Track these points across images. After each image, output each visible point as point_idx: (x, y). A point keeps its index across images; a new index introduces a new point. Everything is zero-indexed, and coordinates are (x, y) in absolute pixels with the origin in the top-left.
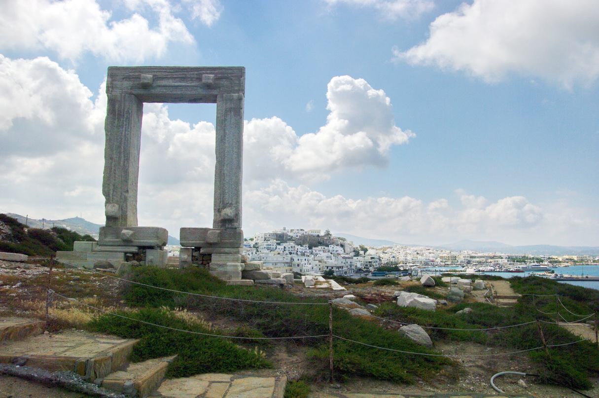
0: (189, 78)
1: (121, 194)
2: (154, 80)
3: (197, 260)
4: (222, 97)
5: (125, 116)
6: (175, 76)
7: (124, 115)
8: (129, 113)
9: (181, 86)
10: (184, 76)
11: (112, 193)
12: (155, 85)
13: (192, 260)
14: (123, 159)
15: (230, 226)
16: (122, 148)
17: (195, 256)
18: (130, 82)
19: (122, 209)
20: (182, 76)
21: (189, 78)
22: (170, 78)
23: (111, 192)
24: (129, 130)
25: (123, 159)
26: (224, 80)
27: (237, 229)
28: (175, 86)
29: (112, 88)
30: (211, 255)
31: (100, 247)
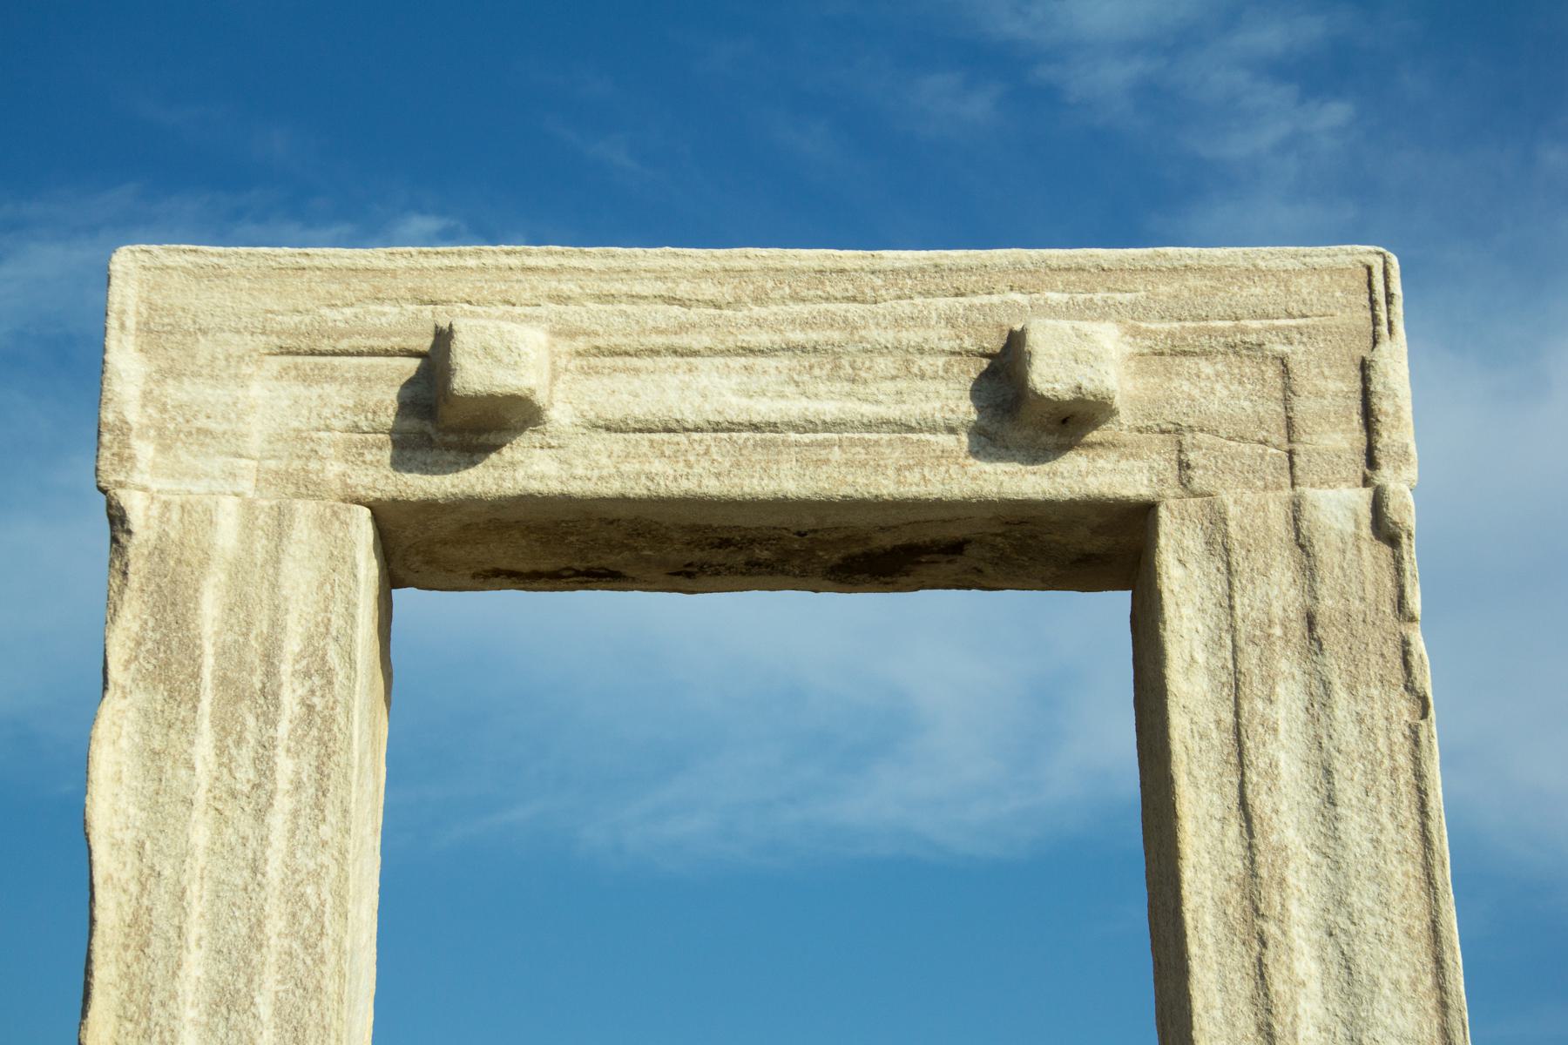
0: (884, 350)
2: (555, 377)
4: (1217, 520)
6: (763, 339)
7: (270, 695)
8: (327, 675)
9: (809, 426)
10: (836, 336)
12: (559, 414)
16: (265, 1010)
18: (330, 389)
20: (814, 336)
21: (884, 350)
22: (713, 352)
24: (325, 830)
26: (1206, 368)
28: (755, 427)
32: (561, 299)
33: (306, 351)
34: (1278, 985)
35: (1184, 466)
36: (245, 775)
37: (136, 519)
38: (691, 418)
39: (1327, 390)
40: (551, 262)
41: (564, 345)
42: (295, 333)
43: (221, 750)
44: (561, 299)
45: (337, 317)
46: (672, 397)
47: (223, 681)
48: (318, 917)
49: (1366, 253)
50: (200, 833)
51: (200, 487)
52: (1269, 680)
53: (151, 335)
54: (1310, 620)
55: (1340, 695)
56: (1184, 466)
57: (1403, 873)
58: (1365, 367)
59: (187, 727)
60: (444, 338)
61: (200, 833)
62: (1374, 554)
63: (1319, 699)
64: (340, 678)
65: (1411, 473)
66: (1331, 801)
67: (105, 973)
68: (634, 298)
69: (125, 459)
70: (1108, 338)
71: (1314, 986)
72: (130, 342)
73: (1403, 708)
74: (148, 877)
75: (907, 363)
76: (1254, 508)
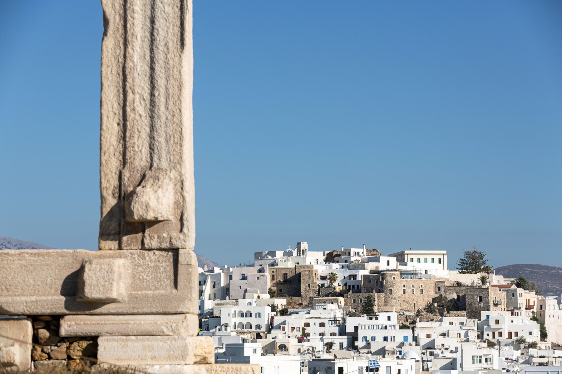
3: (50, 358)
13: (33, 359)
15: (155, 244)
27: (181, 251)
30: (93, 340)
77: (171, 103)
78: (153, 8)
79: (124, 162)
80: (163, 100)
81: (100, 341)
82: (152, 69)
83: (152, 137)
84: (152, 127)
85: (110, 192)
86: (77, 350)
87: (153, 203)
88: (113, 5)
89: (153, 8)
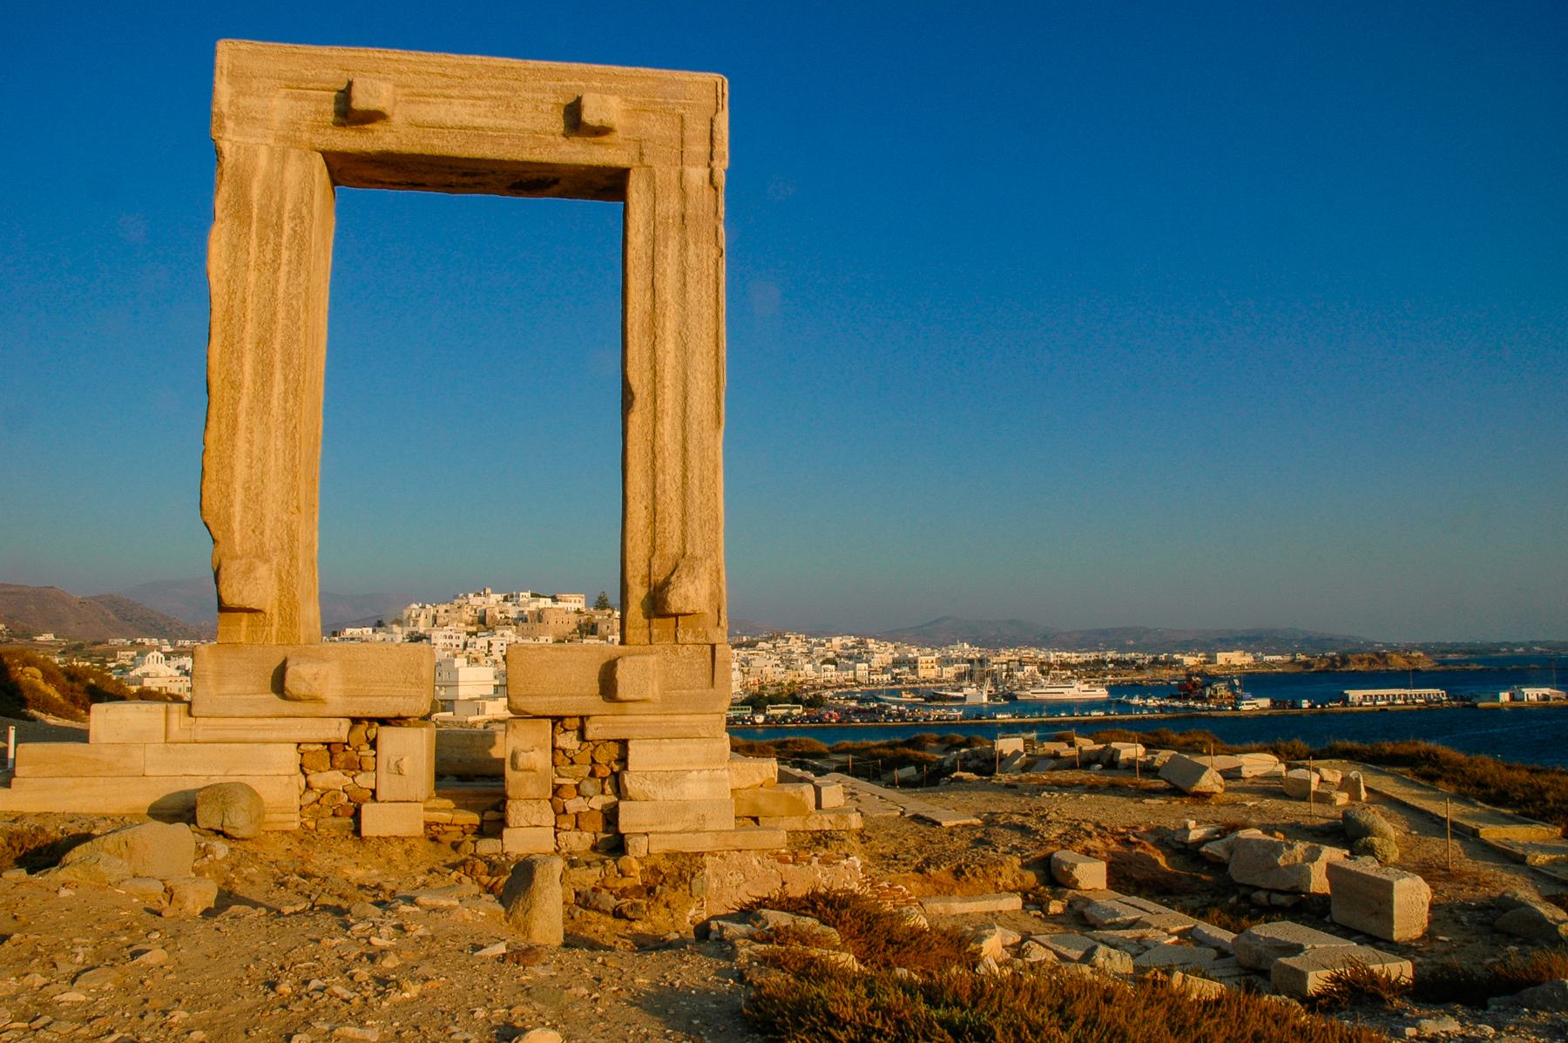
1: (277, 519)
2: (396, 102)
3: (573, 763)
4: (652, 176)
5: (287, 228)
6: (480, 93)
8: (302, 219)
11: (238, 518)
12: (397, 119)
13: (554, 764)
14: (278, 387)
16: (277, 347)
17: (564, 751)
18: (305, 104)
19: (281, 579)
22: (459, 97)
23: (237, 509)
24: (301, 279)
25: (278, 387)
29: (238, 121)
30: (623, 744)
31: (201, 721)
32: (401, 73)
33: (296, 86)
34: (659, 352)
35: (641, 154)
36: (269, 256)
37: (226, 152)
38: (449, 124)
39: (698, 128)
40: (395, 57)
41: (399, 91)
42: (290, 80)
43: (260, 246)
44: (401, 73)
45: (309, 74)
46: (442, 114)
47: (261, 219)
48: (298, 313)
49: (716, 77)
50: (252, 277)
51: (252, 141)
52: (666, 240)
53: (234, 77)
54: (683, 218)
55: (692, 247)
56: (641, 154)
57: (708, 313)
58: (712, 121)
59: (248, 234)
60: (350, 84)
61: (252, 277)
62: (708, 193)
63: (684, 247)
64: (307, 220)
65: (726, 164)
66: (685, 285)
67: (216, 329)
68: (429, 74)
69: (222, 128)
70: (614, 102)
71: (672, 354)
72: (225, 80)
73: (714, 252)
74: (231, 294)
75: (536, 107)
76: (666, 173)
77: (705, 484)
78: (685, 386)
79: (653, 548)
80: (696, 482)
81: (630, 745)
82: (685, 449)
83: (684, 523)
84: (684, 513)
85: (638, 580)
86: (607, 754)
87: (692, 594)
88: (641, 380)
89: (685, 386)
